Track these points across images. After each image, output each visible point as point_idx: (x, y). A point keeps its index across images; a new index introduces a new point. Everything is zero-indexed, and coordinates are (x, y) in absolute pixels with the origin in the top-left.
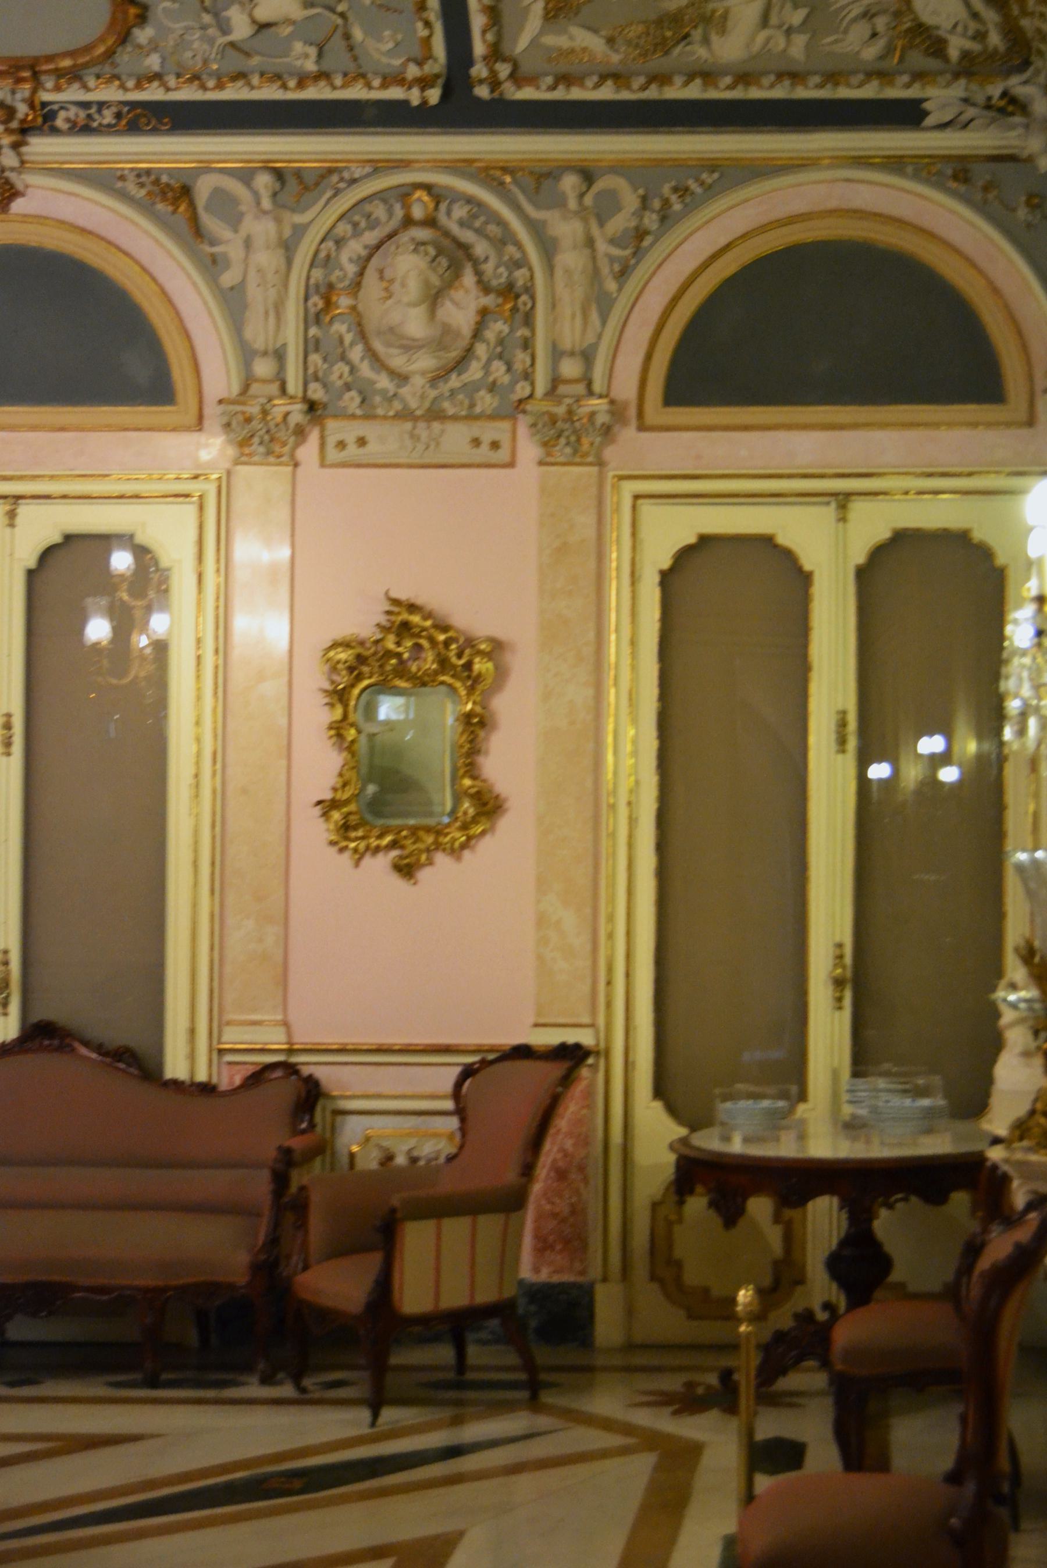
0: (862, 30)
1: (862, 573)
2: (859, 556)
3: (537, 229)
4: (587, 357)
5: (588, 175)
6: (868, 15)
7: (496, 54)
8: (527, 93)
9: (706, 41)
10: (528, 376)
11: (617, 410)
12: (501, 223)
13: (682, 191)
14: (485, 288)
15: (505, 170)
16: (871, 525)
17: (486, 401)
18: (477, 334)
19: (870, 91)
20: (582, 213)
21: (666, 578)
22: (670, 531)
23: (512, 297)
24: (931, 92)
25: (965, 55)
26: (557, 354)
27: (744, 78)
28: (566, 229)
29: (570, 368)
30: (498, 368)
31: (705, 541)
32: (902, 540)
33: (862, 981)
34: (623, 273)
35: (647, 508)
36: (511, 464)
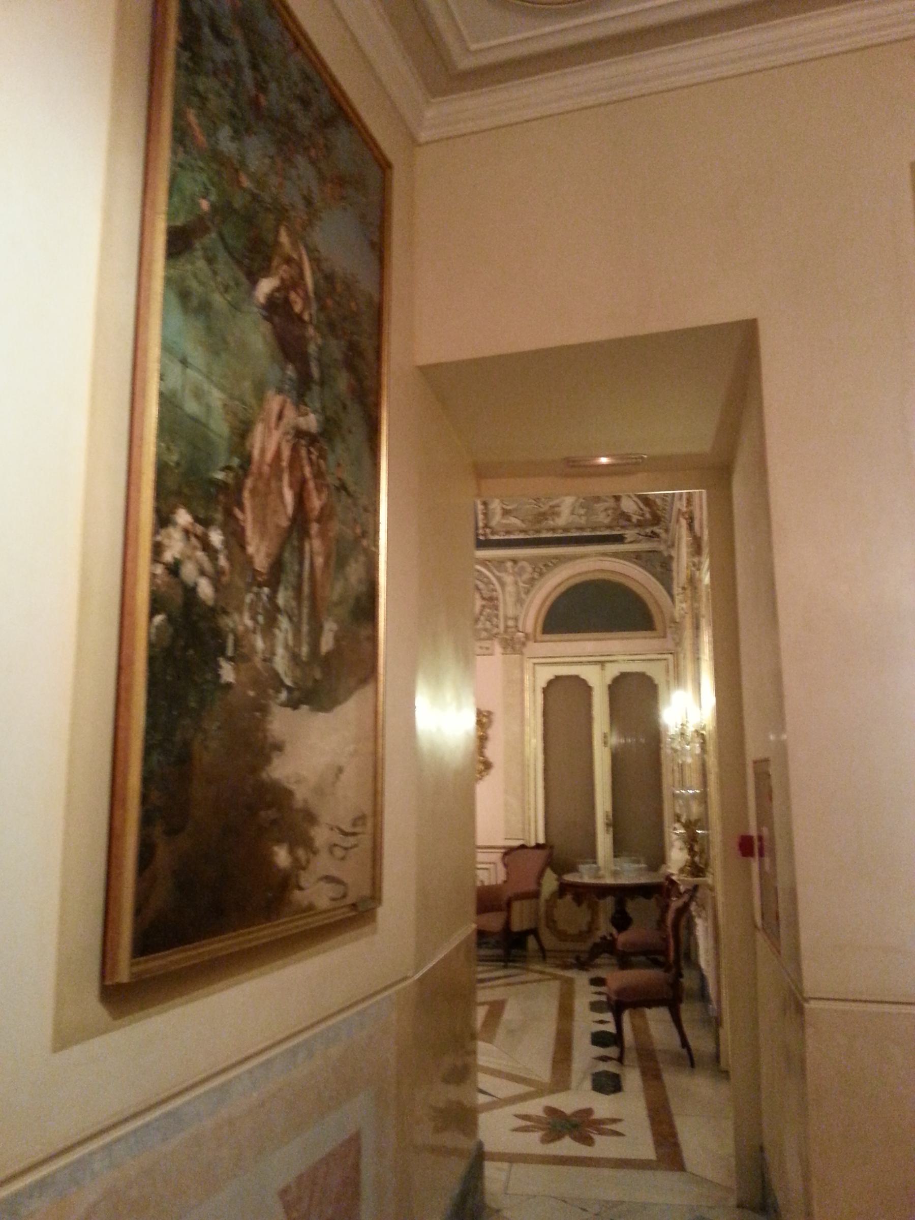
0: (604, 514)
1: (610, 687)
2: (608, 681)
3: (499, 579)
4: (516, 619)
5: (515, 561)
6: (606, 510)
7: (486, 526)
8: (496, 537)
9: (553, 520)
10: (497, 627)
11: (527, 636)
12: (487, 577)
13: (545, 565)
14: (484, 599)
15: (489, 561)
16: (613, 671)
17: (484, 634)
18: (481, 614)
19: (607, 532)
20: (514, 574)
21: (545, 691)
22: (546, 674)
23: (491, 601)
24: (627, 532)
25: (638, 521)
26: (506, 618)
27: (565, 530)
28: (509, 579)
29: (511, 623)
30: (488, 625)
31: (558, 678)
32: (623, 676)
33: (616, 823)
34: (527, 592)
35: (538, 668)
36: (491, 655)
